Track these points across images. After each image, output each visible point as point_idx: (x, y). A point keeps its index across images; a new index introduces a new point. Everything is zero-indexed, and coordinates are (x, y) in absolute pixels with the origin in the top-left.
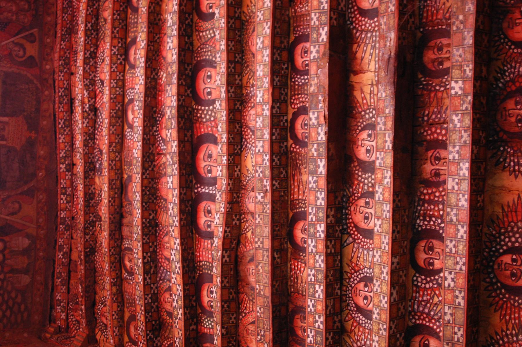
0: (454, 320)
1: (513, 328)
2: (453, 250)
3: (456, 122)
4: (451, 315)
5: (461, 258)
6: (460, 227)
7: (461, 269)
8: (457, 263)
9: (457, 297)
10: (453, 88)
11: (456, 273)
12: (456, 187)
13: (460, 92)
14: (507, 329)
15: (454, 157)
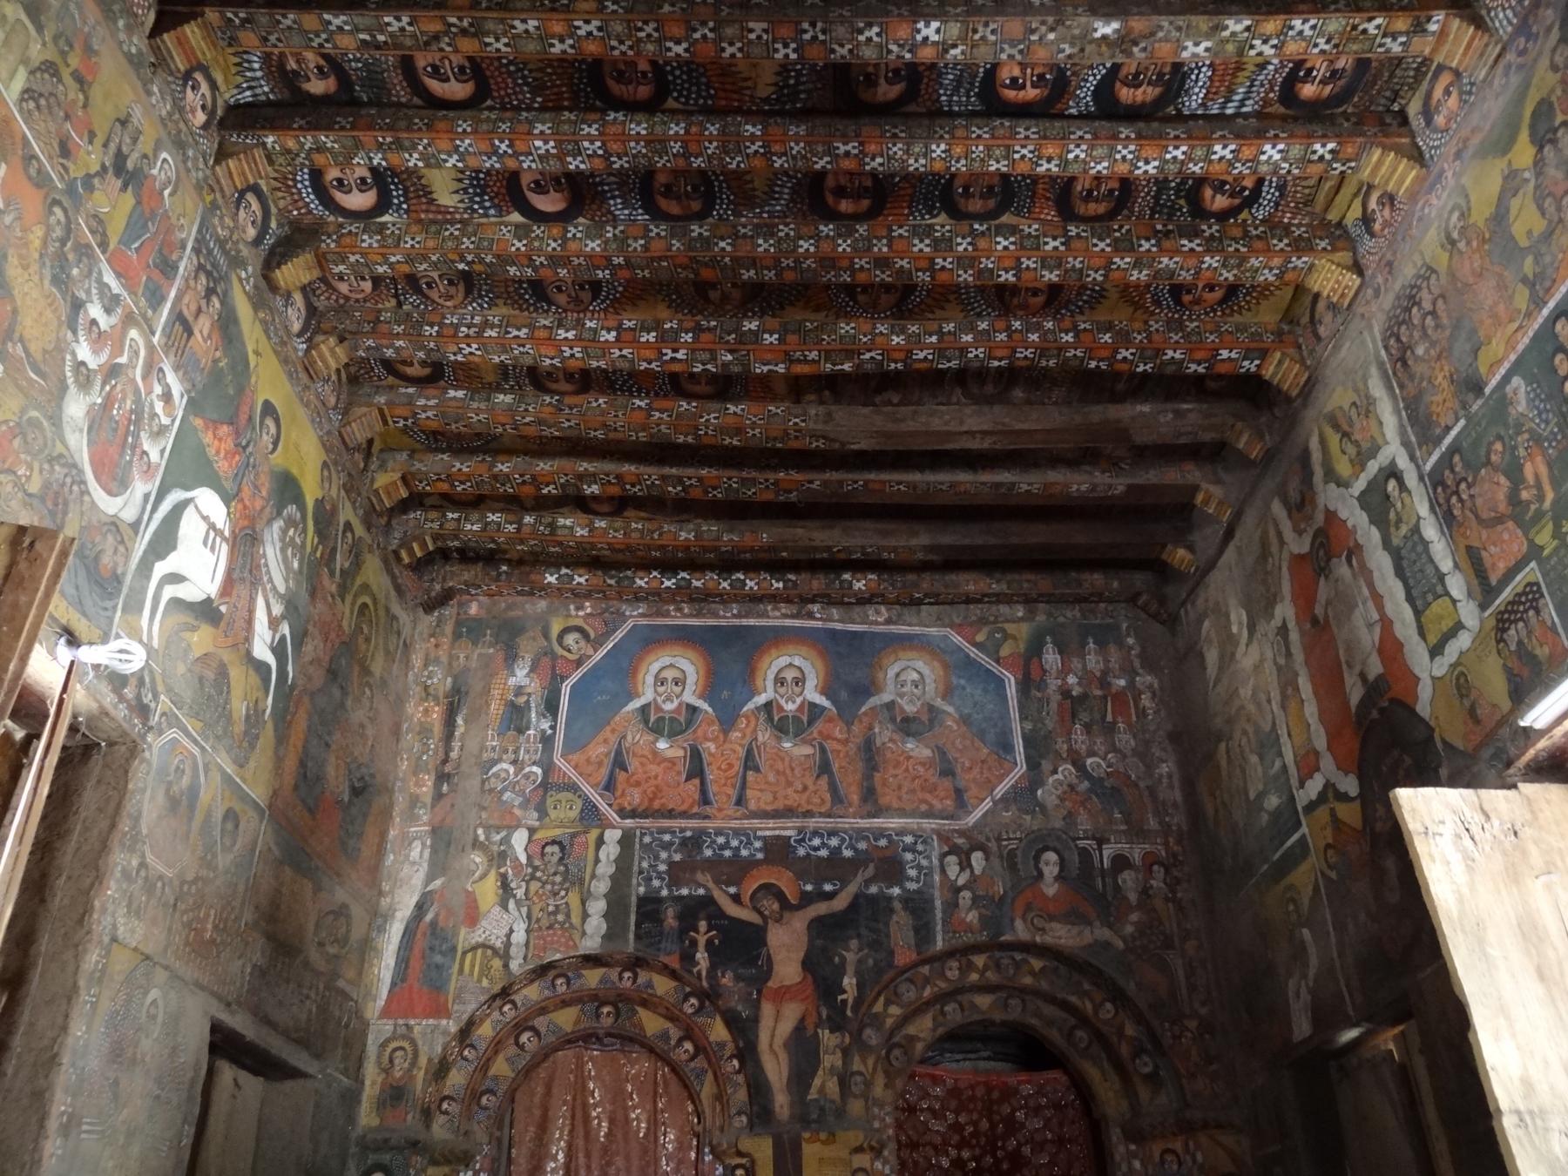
0: (519, 36)
1: (535, 79)
2: (642, 34)
3: (867, 34)
4: (527, 31)
5: (631, 48)
6: (685, 45)
7: (613, 48)
8: (622, 42)
9: (562, 41)
10: (927, 25)
11: (602, 38)
12: (752, 36)
13: (919, 38)
14: (530, 71)
15: (806, 31)
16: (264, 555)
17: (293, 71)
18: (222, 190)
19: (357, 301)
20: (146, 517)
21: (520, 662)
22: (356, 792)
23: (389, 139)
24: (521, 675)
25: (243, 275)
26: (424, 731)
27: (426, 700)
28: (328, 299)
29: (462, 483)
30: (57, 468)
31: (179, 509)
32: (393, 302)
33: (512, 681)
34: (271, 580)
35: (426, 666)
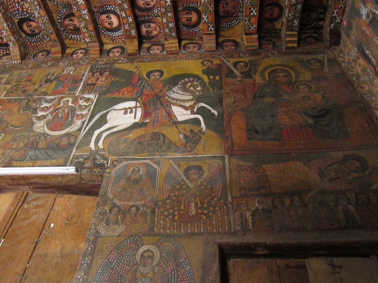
16: (169, 97)
17: (74, 27)
18: (97, 58)
19: (160, 30)
20: (85, 125)
21: (361, 9)
22: (315, 117)
23: (75, 7)
24: (364, 12)
25: (120, 61)
26: (364, 70)
27: (357, 62)
28: (161, 38)
29: (252, 11)
30: (31, 138)
31: (105, 115)
32: (158, 18)
33: (364, 17)
34: (177, 100)
35: (349, 55)
